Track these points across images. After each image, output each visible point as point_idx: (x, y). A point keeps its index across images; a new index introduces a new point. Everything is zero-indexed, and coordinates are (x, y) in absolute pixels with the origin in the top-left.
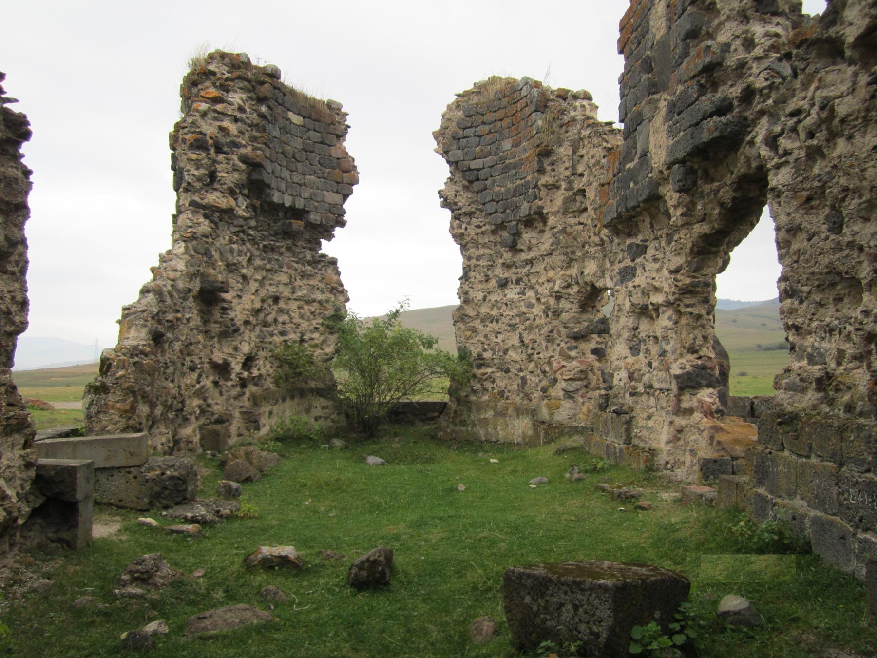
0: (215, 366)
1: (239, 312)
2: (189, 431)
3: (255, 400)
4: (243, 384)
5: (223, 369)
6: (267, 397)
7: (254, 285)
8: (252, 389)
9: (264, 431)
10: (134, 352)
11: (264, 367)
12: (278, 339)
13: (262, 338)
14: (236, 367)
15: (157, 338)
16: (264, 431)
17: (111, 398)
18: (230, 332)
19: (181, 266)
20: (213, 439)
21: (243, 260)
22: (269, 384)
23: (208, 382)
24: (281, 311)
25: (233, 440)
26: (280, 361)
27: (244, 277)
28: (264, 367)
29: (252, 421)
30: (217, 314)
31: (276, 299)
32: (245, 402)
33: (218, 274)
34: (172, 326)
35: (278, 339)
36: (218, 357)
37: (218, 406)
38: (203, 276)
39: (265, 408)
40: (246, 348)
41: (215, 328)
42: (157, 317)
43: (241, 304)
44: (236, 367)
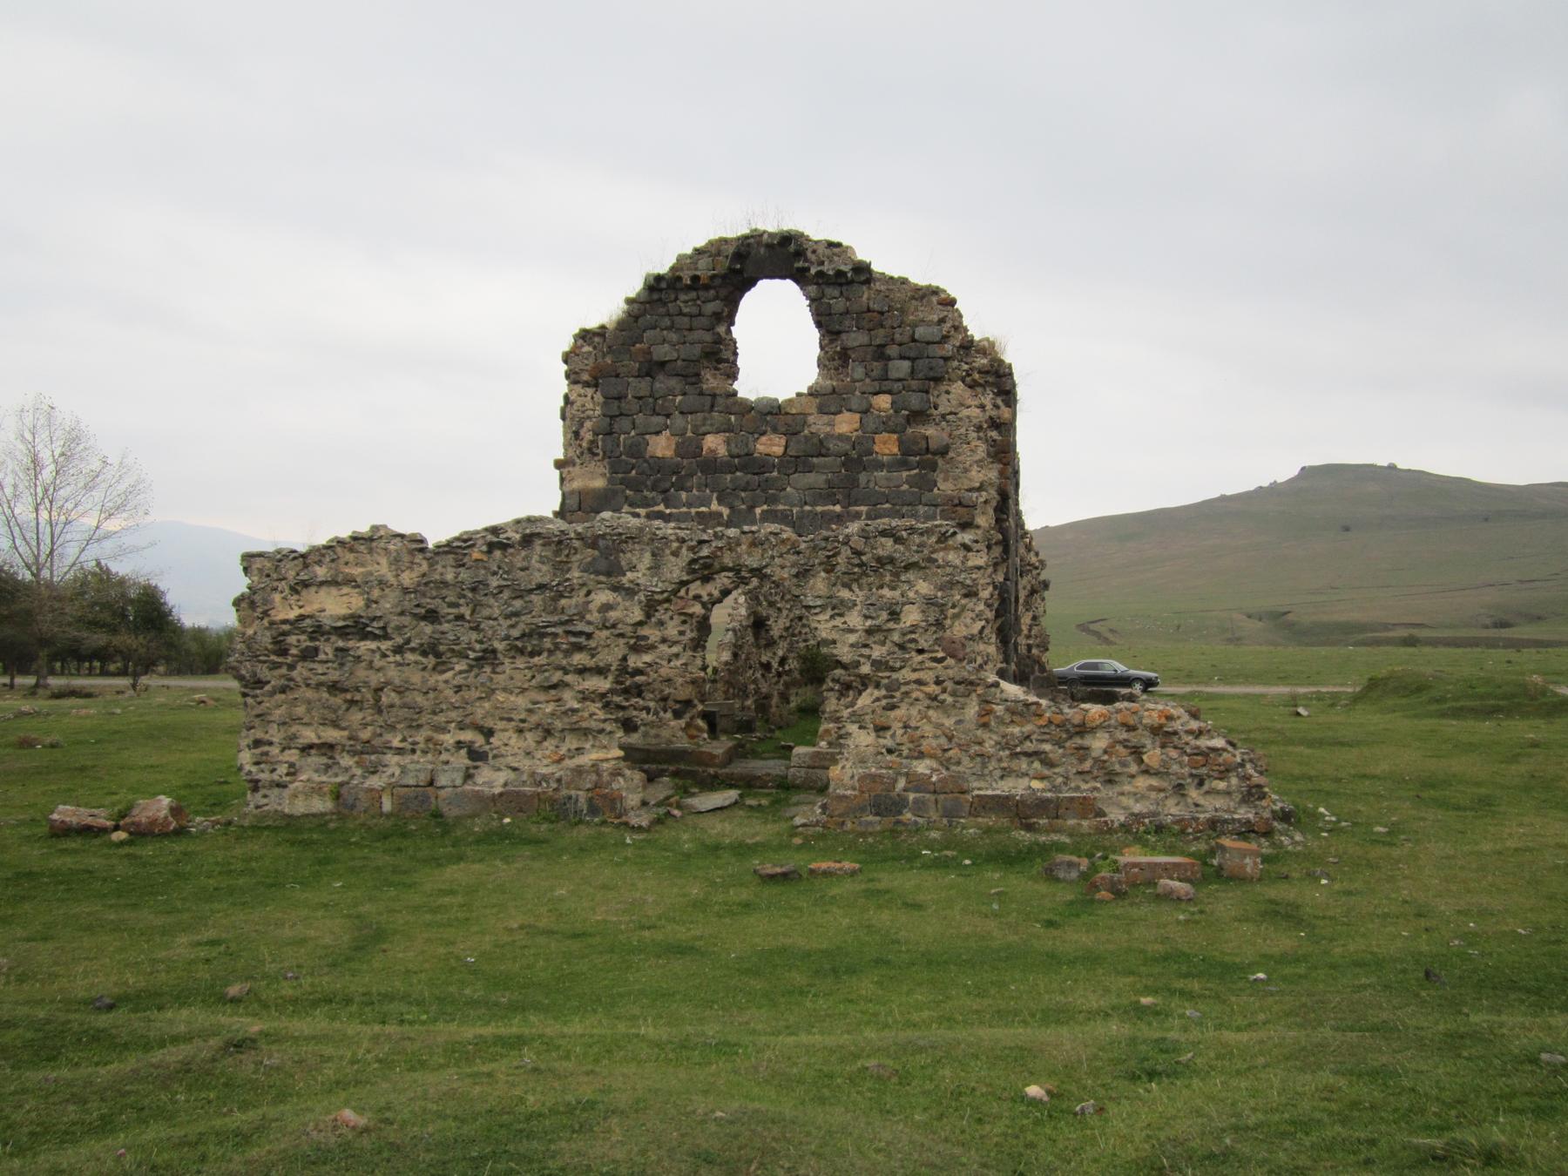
0: (762, 665)
1: (776, 632)
2: (749, 702)
3: (787, 685)
4: (779, 675)
5: (767, 667)
6: (794, 683)
7: (785, 612)
8: (785, 678)
9: (793, 705)
10: (726, 663)
11: (793, 664)
12: (802, 645)
13: (791, 644)
14: (775, 665)
15: (735, 655)
16: (793, 705)
17: (719, 685)
18: (771, 643)
19: (743, 611)
20: (763, 705)
21: (778, 598)
22: (796, 675)
23: (758, 675)
24: (804, 626)
25: (773, 710)
26: (803, 659)
27: (779, 609)
28: (793, 664)
29: (785, 698)
30: (763, 633)
31: (800, 618)
32: (781, 687)
33: (763, 610)
34: (741, 647)
35: (802, 645)
36: (764, 659)
37: (764, 689)
38: (755, 613)
39: (793, 691)
40: (780, 653)
41: (763, 642)
42: (735, 645)
43: (777, 627)
44: (775, 665)
